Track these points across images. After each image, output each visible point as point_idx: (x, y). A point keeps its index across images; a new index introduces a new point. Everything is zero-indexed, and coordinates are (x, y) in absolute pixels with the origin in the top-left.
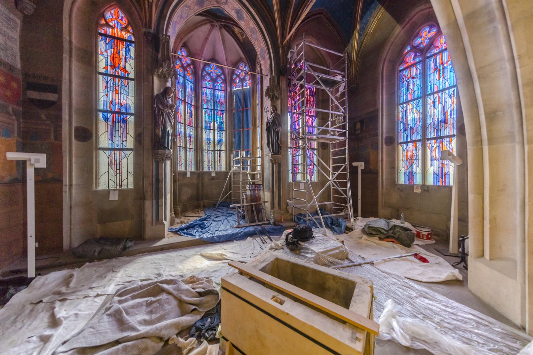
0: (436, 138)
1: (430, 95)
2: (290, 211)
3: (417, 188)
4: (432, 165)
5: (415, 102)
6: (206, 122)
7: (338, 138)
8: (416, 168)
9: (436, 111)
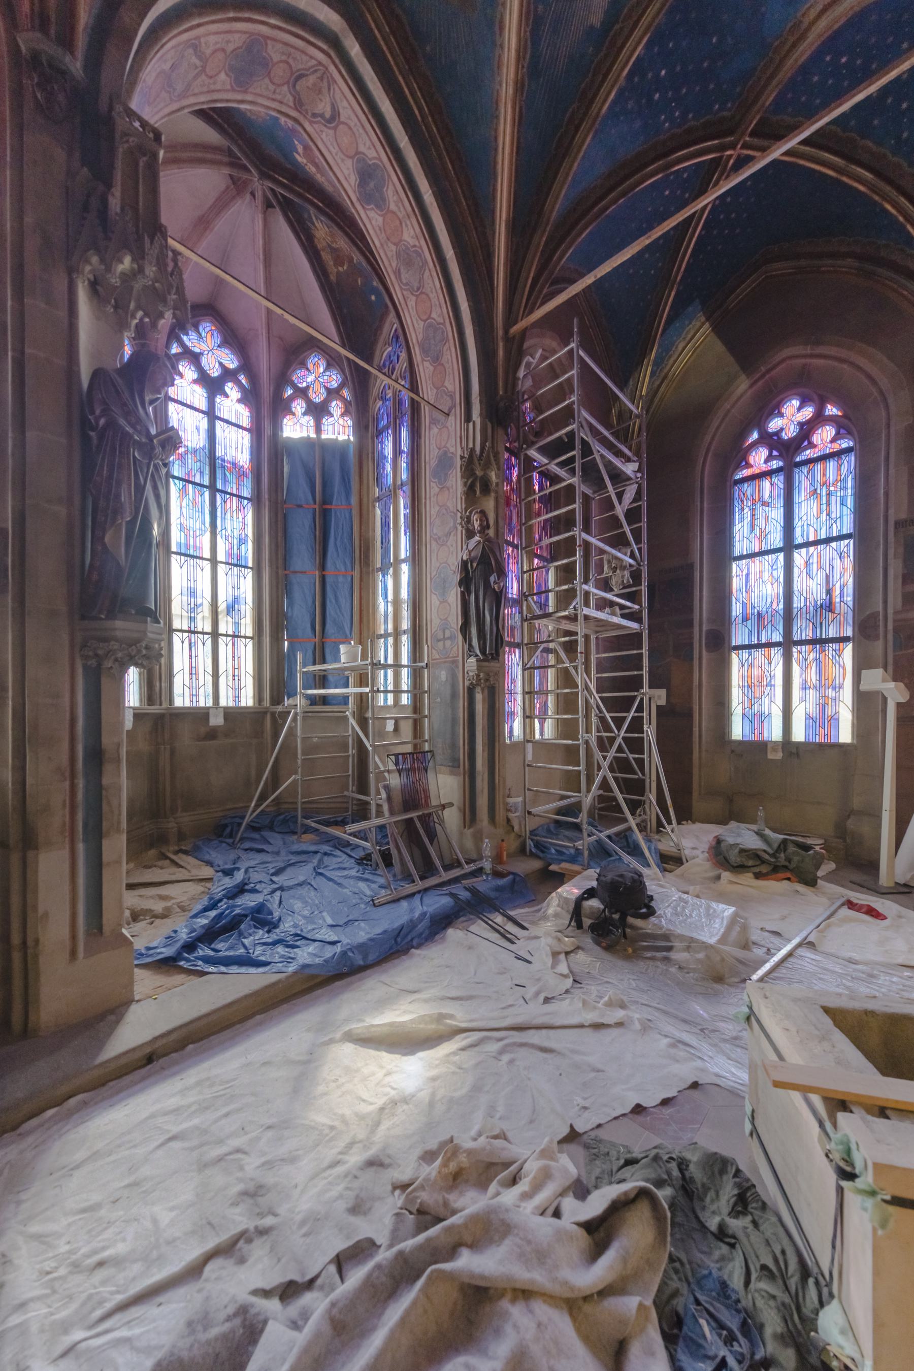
0: (812, 642)
1: (800, 546)
2: (516, 828)
3: (774, 750)
4: (803, 700)
5: (769, 558)
6: (182, 528)
7: (624, 622)
8: (770, 706)
9: (813, 584)
